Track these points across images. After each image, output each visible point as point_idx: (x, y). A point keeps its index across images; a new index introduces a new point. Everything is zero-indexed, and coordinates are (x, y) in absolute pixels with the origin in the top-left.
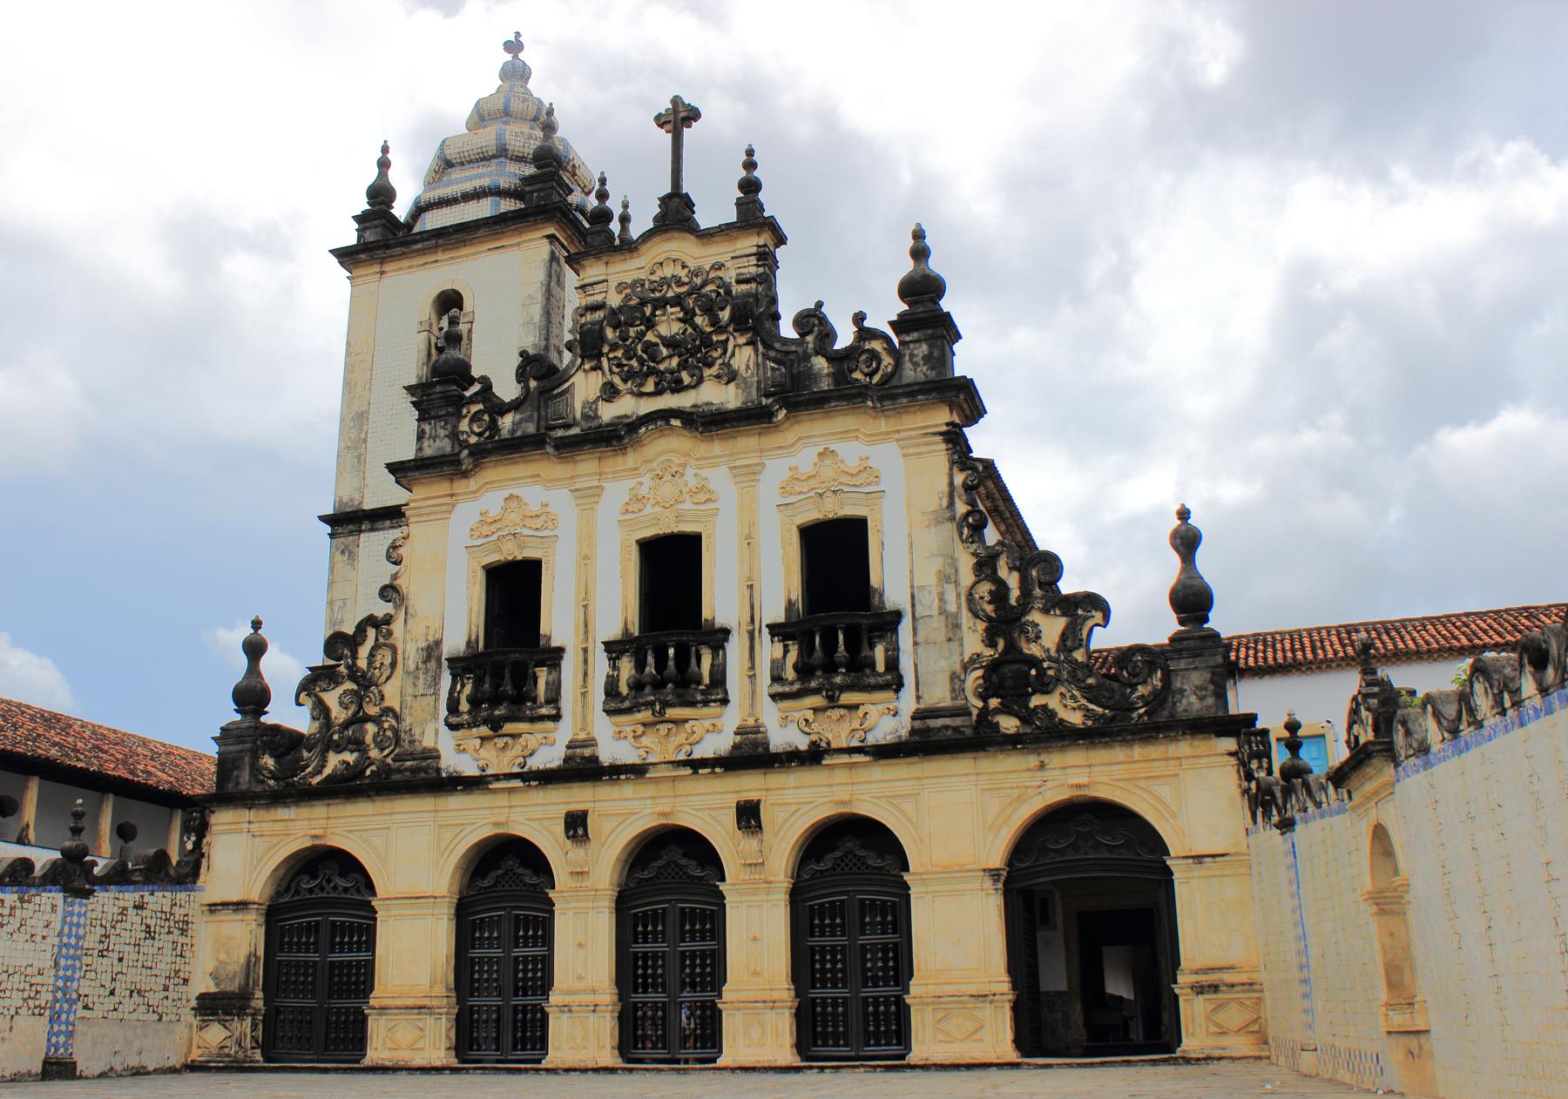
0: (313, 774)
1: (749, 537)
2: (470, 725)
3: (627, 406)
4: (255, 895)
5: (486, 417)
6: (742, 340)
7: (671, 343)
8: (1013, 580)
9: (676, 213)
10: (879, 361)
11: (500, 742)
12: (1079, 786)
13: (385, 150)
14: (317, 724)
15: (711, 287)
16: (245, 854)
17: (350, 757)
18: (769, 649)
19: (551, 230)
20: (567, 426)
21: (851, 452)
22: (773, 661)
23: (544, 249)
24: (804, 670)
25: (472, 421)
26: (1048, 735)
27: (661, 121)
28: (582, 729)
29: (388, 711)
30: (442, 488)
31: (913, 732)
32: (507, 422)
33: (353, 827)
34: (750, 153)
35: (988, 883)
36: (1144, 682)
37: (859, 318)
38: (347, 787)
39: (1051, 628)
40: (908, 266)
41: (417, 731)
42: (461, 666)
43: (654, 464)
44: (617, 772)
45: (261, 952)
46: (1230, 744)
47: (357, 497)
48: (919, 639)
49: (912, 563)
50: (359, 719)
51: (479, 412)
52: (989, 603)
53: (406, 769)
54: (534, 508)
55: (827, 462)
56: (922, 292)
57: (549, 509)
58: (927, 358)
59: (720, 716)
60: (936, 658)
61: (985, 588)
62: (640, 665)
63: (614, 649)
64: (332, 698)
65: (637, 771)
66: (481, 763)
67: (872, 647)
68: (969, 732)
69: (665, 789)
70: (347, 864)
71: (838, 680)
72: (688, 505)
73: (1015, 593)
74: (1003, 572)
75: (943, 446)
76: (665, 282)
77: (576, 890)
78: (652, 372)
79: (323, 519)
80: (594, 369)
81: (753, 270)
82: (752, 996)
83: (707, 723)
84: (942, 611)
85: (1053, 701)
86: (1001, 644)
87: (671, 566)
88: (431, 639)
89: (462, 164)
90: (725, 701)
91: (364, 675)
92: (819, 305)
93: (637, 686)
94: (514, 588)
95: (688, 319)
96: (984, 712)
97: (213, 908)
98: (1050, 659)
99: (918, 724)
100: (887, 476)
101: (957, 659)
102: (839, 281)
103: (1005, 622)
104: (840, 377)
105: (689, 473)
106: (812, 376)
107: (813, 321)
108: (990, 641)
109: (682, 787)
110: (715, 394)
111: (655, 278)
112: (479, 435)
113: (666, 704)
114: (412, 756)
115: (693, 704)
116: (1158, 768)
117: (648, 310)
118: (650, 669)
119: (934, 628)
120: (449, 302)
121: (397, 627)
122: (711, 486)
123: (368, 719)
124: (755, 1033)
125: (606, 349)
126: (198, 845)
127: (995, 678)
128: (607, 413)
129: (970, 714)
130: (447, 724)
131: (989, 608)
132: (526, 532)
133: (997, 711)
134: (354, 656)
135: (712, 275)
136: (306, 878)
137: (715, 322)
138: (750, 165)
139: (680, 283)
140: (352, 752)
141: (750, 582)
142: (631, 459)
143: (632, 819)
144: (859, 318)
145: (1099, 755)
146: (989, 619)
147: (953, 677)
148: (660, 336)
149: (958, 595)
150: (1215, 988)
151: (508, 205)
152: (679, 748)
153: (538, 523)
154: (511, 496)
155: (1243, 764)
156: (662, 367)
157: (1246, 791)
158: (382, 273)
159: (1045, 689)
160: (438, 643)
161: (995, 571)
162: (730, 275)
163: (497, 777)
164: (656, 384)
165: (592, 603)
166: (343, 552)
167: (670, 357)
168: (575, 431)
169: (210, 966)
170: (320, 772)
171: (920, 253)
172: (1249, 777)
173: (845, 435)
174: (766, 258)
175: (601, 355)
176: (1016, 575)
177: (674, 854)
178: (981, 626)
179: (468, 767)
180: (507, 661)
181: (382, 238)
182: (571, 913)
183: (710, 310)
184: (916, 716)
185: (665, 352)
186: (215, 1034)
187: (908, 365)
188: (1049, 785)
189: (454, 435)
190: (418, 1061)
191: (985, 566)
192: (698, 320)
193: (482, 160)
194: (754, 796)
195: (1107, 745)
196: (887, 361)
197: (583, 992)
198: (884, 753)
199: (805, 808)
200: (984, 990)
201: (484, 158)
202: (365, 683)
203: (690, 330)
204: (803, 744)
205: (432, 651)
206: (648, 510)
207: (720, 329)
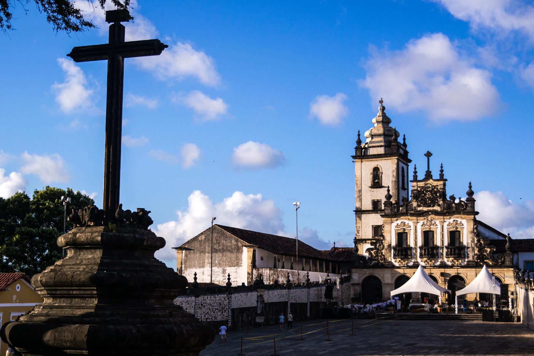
4: (360, 282)
7: (429, 198)
8: (483, 242)
9: (429, 175)
13: (359, 132)
21: (459, 220)
23: (396, 161)
40: (468, 189)
42: (395, 249)
46: (512, 269)
49: (467, 238)
56: (471, 193)
58: (471, 206)
60: (471, 255)
62: (425, 251)
63: (421, 248)
64: (373, 252)
70: (376, 278)
72: (432, 226)
87: (428, 235)
94: (402, 236)
95: (432, 194)
97: (353, 284)
102: (457, 191)
103: (481, 249)
104: (456, 208)
105: (433, 222)
106: (452, 207)
107: (453, 198)
108: (479, 251)
110: (437, 208)
116: (502, 272)
119: (470, 249)
120: (376, 170)
128: (419, 209)
138: (442, 167)
142: (422, 218)
146: (479, 248)
147: (473, 257)
151: (389, 151)
158: (362, 162)
160: (391, 245)
162: (439, 188)
171: (470, 187)
173: (458, 217)
174: (444, 185)
189: (391, 210)
191: (479, 241)
198: (462, 267)
201: (379, 135)
202: (378, 250)
205: (390, 246)
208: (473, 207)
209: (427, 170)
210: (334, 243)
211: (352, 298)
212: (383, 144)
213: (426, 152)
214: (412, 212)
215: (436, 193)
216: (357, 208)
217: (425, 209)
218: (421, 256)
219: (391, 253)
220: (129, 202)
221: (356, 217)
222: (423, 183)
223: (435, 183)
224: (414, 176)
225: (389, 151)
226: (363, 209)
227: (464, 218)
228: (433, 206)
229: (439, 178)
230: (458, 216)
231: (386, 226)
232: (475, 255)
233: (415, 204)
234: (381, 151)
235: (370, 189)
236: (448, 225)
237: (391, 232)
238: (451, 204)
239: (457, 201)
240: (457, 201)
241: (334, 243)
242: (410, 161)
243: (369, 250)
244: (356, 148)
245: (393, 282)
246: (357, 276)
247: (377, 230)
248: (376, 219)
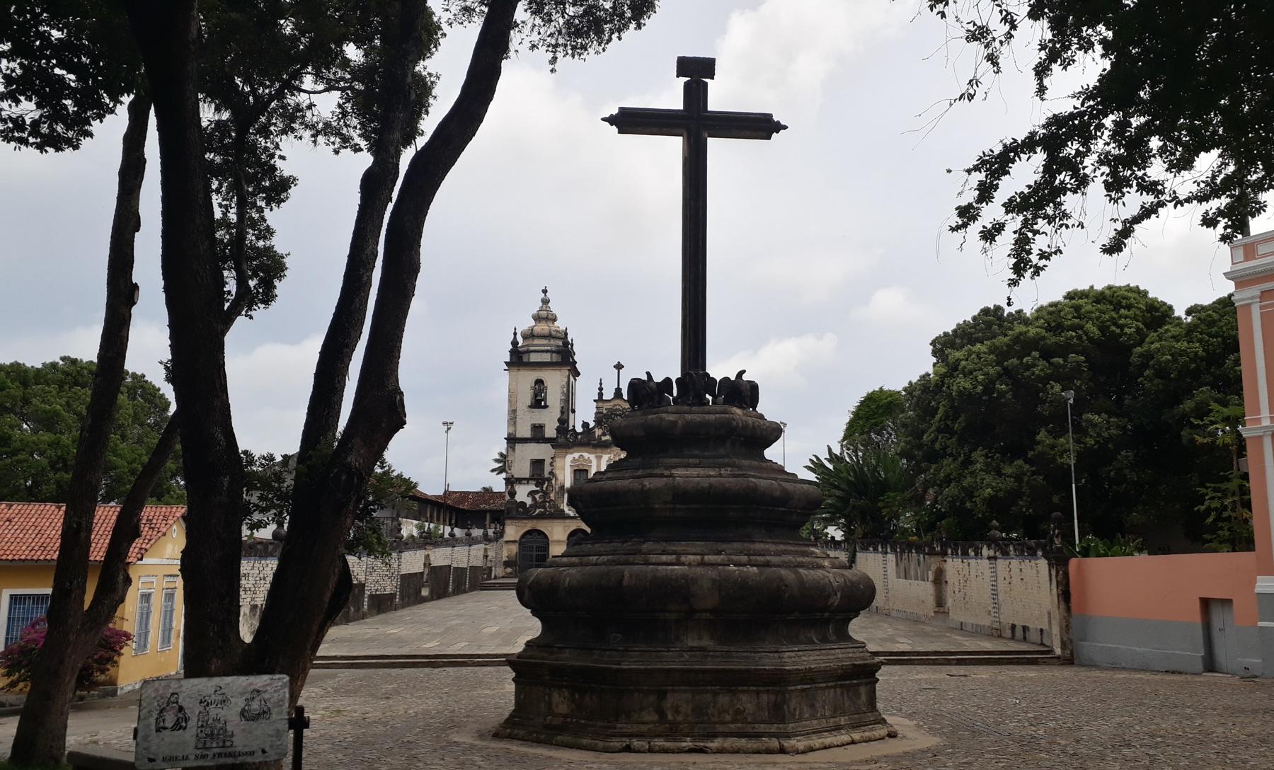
9: (618, 393)
16: (513, 531)
33: (543, 526)
38: (542, 517)
42: (569, 491)
50: (545, 502)
64: (537, 496)
120: (539, 382)
151: (556, 358)
179: (572, 514)
181: (518, 359)
186: (509, 570)
202: (545, 494)
220: (719, 368)
225: (556, 358)
233: (598, 432)
234: (546, 358)
242: (578, 374)
243: (532, 494)
244: (511, 352)
245: (565, 538)
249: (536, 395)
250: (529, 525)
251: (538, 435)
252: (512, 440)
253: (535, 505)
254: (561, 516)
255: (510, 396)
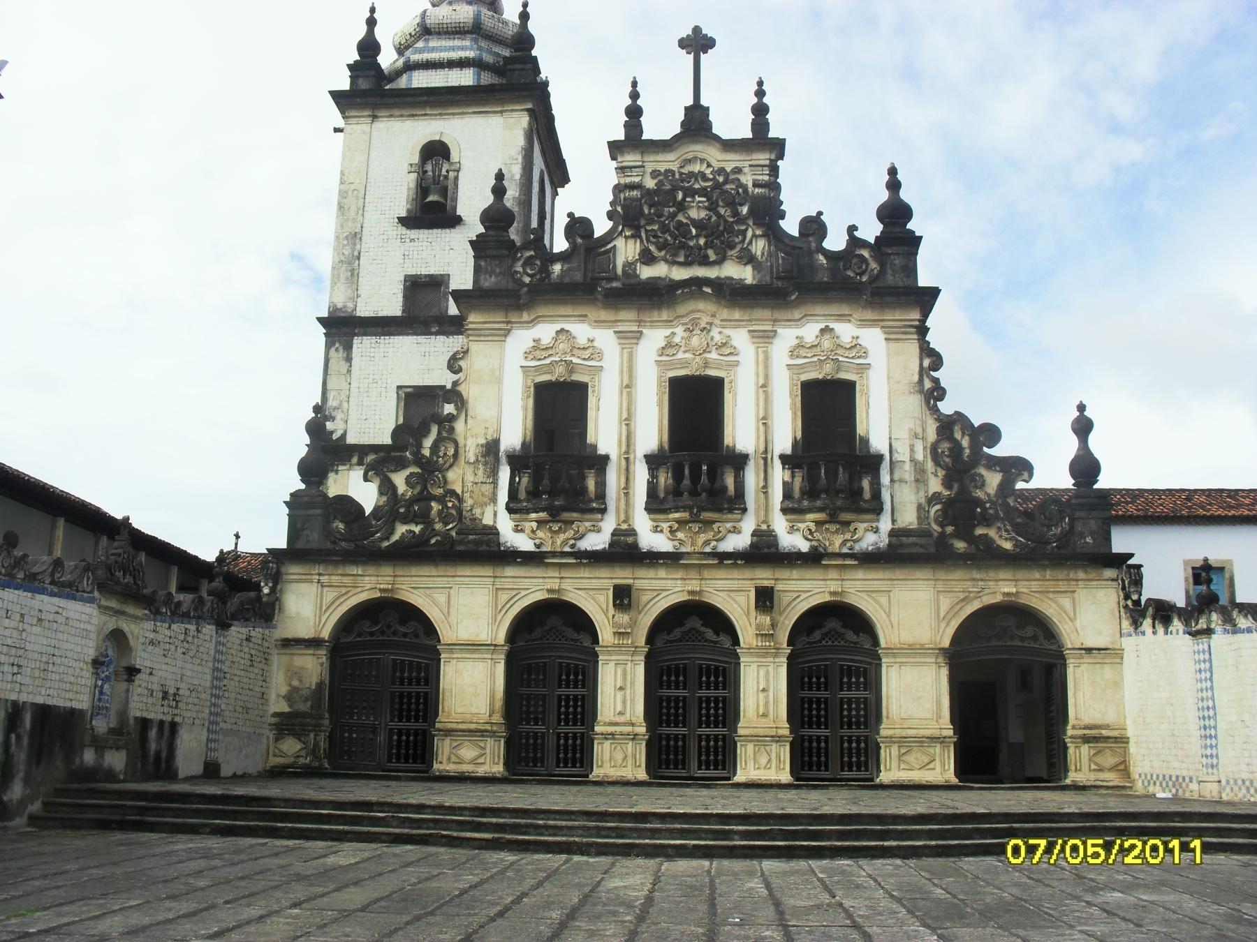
0: (382, 539)
1: (764, 386)
2: (528, 511)
3: (659, 270)
5: (538, 263)
6: (758, 232)
8: (965, 442)
9: (696, 122)
10: (868, 265)
11: (556, 527)
12: (1009, 594)
13: (373, 10)
14: (384, 498)
15: (728, 187)
17: (417, 529)
18: (779, 475)
19: (530, 106)
20: (610, 280)
21: (845, 331)
22: (785, 483)
24: (811, 492)
25: (524, 266)
26: (986, 557)
27: (683, 44)
28: (624, 522)
29: (453, 493)
30: (499, 317)
31: (890, 545)
32: (557, 268)
34: (760, 83)
35: (940, 660)
36: (1056, 526)
37: (852, 229)
38: (414, 553)
39: (993, 480)
41: (477, 511)
42: (517, 462)
43: (685, 320)
44: (653, 559)
45: (327, 682)
46: (1110, 573)
47: (350, 305)
48: (896, 477)
50: (424, 498)
51: (531, 257)
52: (948, 456)
53: (469, 542)
54: (582, 341)
55: (827, 336)
56: (895, 214)
57: (595, 344)
59: (740, 520)
61: (945, 446)
62: (678, 476)
63: (653, 461)
64: (399, 480)
65: (671, 559)
66: (537, 541)
67: (860, 480)
68: (932, 550)
69: (693, 574)
71: (839, 503)
72: (713, 355)
73: (967, 451)
74: (958, 435)
75: (915, 337)
76: (691, 175)
77: (619, 646)
78: (684, 246)
79: (319, 319)
80: (633, 236)
81: (766, 178)
82: (761, 732)
83: (729, 525)
84: (912, 460)
85: (992, 533)
86: (956, 486)
87: (696, 404)
88: (490, 438)
89: (439, 33)
90: (745, 510)
91: (429, 461)
92: (820, 213)
93: (676, 492)
94: (560, 404)
95: (712, 208)
96: (943, 535)
98: (990, 501)
99: (894, 539)
100: (873, 353)
101: (922, 494)
105: (715, 332)
107: (814, 226)
108: (947, 483)
109: (706, 574)
111: (685, 171)
112: (531, 276)
113: (702, 509)
114: (474, 531)
115: (720, 510)
116: (1063, 586)
117: (680, 196)
118: (686, 482)
119: (907, 472)
120: (435, 152)
121: (459, 426)
122: (734, 343)
123: (434, 498)
124: (763, 760)
125: (643, 222)
126: (273, 590)
127: (950, 512)
128: (646, 272)
129: (931, 536)
130: (510, 510)
131: (947, 460)
132: (575, 360)
133: (953, 535)
134: (419, 446)
135: (732, 177)
136: (368, 623)
137: (736, 214)
139: (707, 180)
140: (417, 524)
141: (761, 420)
142: (665, 315)
143: (664, 594)
144: (852, 229)
145: (1020, 574)
147: (920, 507)
148: (689, 218)
149: (925, 448)
150: (1096, 739)
152: (707, 543)
153: (586, 354)
154: (562, 330)
155: (1123, 588)
156: (691, 244)
157: (1126, 607)
158: (374, 117)
159: (987, 521)
161: (952, 433)
162: (747, 179)
163: (553, 554)
164: (686, 257)
165: (627, 421)
166: (337, 350)
167: (698, 236)
168: (614, 284)
169: (284, 690)
170: (388, 538)
171: (894, 185)
172: (1127, 597)
173: (840, 318)
174: (774, 170)
175: (637, 228)
176: (967, 438)
177: (695, 622)
178: (941, 473)
179: (525, 544)
180: (557, 463)
181: (371, 89)
182: (612, 664)
183: (733, 204)
184: (893, 533)
185: (694, 231)
186: (291, 746)
187: (889, 272)
188: (987, 591)
190: (481, 771)
192: (722, 211)
193: (457, 33)
194: (766, 583)
195: (1028, 567)
196: (874, 265)
197: (625, 724)
199: (804, 596)
200: (936, 733)
202: (430, 470)
203: (714, 218)
204: (804, 546)
205: (491, 448)
206: (680, 355)
207: (742, 220)
208: (912, 271)
209: (690, 102)
210: (237, 536)
211: (276, 715)
212: (470, 54)
213: (687, 31)
214: (614, 284)
215: (733, 204)
216: (333, 310)
217: (680, 274)
218: (655, 505)
219: (495, 483)
221: (329, 346)
222: (671, 156)
223: (730, 161)
224: (626, 125)
226: (364, 311)
227: (873, 323)
228: (719, 262)
229: (749, 134)
230: (845, 309)
231: (474, 347)
232: (934, 499)
233: (626, 250)
234: (465, 78)
235: (404, 231)
236: (793, 353)
237: (499, 381)
238: (811, 254)
239: (835, 241)
240: (835, 241)
241: (237, 536)
245: (501, 637)
246: (312, 606)
247: (426, 409)
248: (418, 360)
249: (422, 189)
250: (366, 584)
251: (425, 307)
252: (342, 328)
253: (392, 510)
254: (484, 551)
255: (343, 194)
